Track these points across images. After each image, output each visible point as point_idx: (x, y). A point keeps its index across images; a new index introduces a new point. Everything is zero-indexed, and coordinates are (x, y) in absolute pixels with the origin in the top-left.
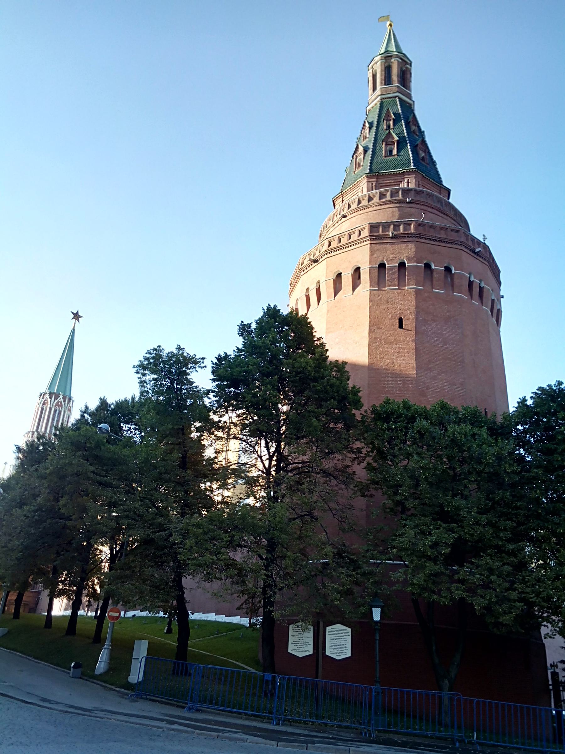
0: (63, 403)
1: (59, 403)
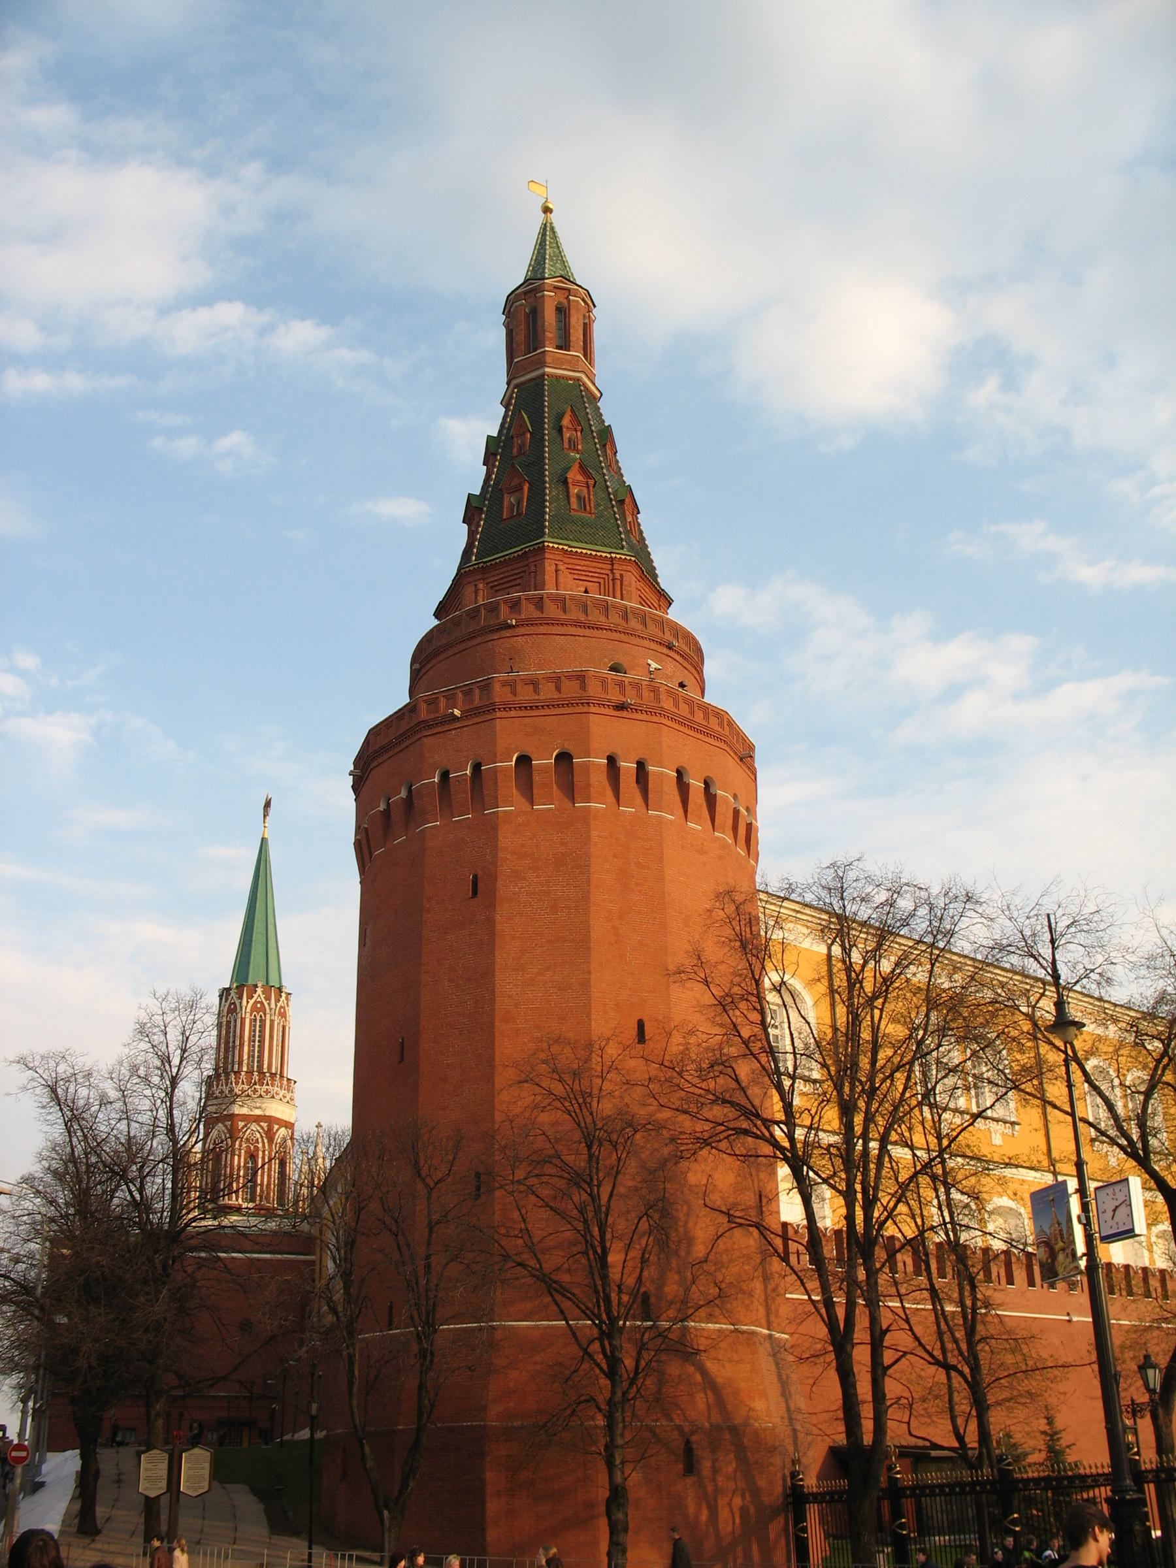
1: (259, 1005)
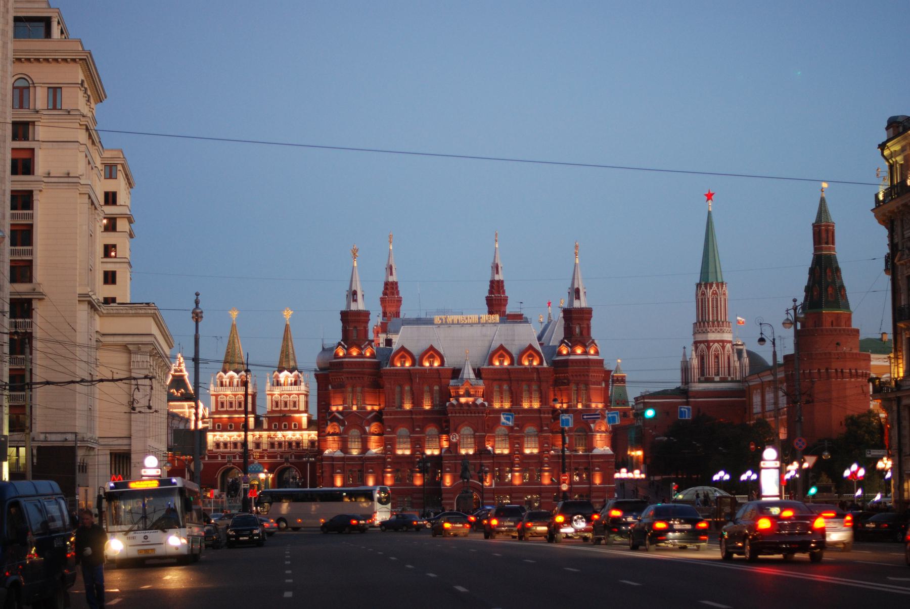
0: (718, 292)
1: (715, 292)
